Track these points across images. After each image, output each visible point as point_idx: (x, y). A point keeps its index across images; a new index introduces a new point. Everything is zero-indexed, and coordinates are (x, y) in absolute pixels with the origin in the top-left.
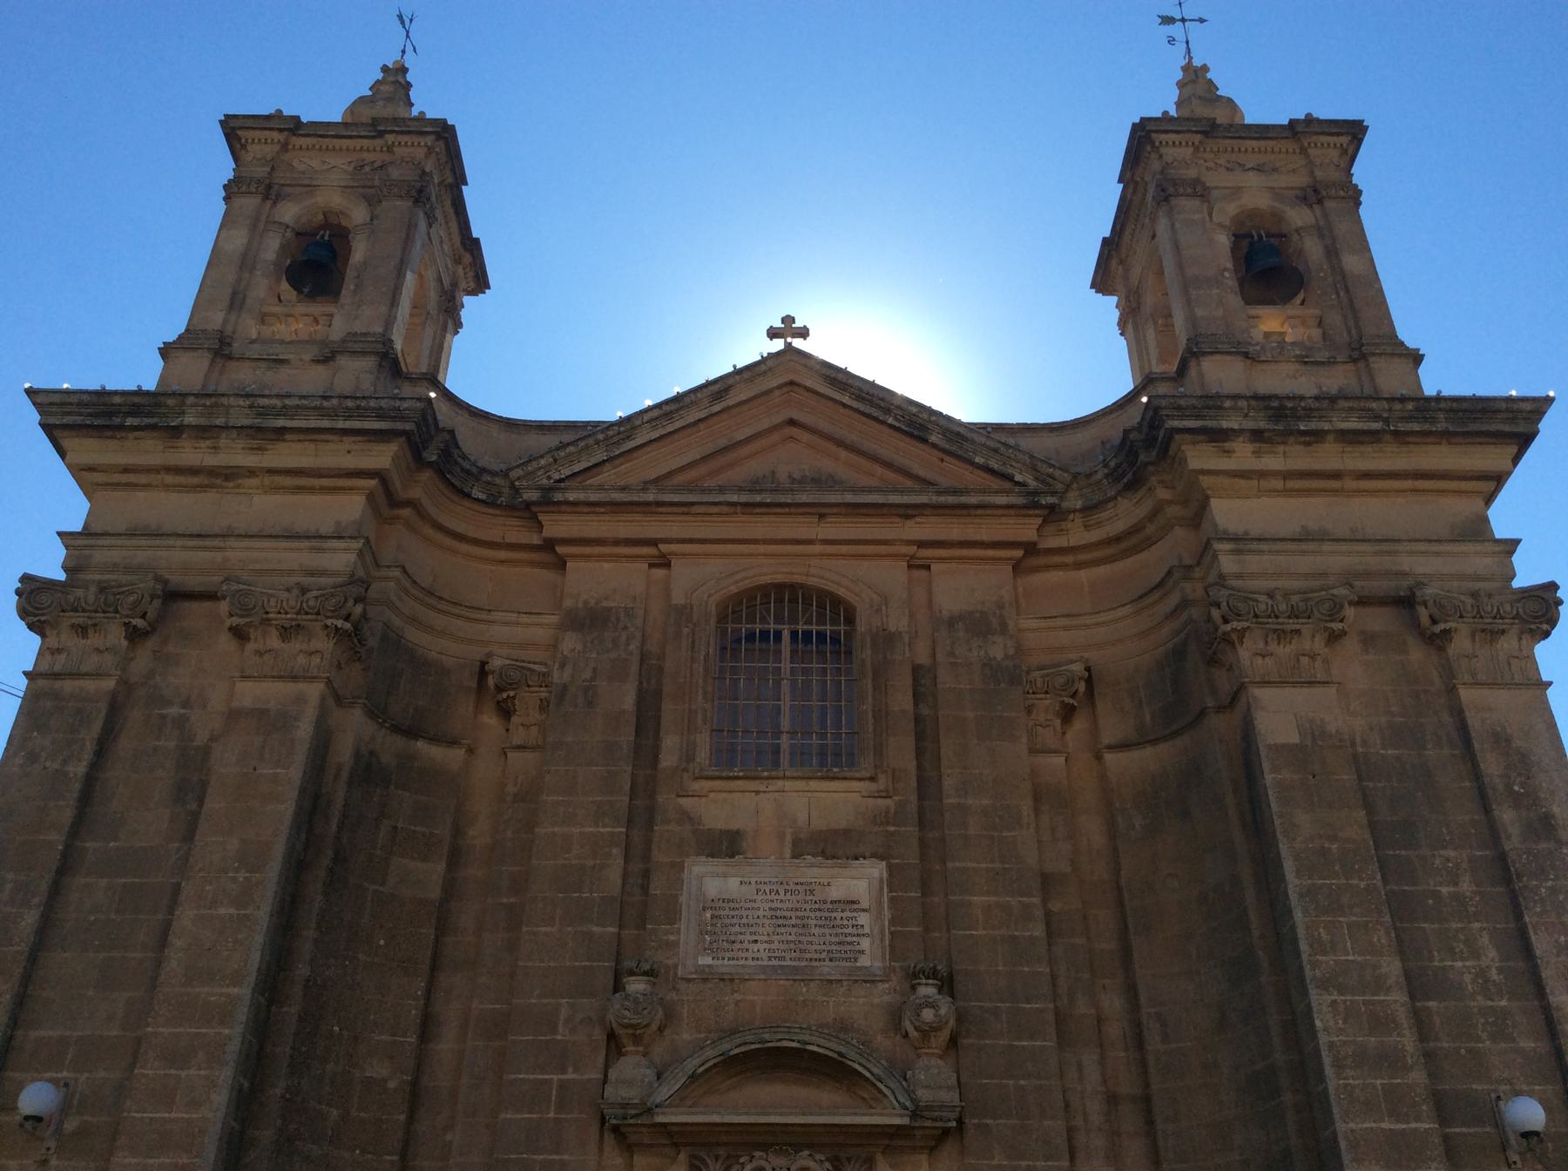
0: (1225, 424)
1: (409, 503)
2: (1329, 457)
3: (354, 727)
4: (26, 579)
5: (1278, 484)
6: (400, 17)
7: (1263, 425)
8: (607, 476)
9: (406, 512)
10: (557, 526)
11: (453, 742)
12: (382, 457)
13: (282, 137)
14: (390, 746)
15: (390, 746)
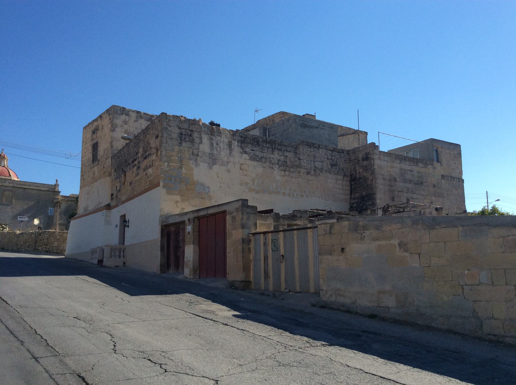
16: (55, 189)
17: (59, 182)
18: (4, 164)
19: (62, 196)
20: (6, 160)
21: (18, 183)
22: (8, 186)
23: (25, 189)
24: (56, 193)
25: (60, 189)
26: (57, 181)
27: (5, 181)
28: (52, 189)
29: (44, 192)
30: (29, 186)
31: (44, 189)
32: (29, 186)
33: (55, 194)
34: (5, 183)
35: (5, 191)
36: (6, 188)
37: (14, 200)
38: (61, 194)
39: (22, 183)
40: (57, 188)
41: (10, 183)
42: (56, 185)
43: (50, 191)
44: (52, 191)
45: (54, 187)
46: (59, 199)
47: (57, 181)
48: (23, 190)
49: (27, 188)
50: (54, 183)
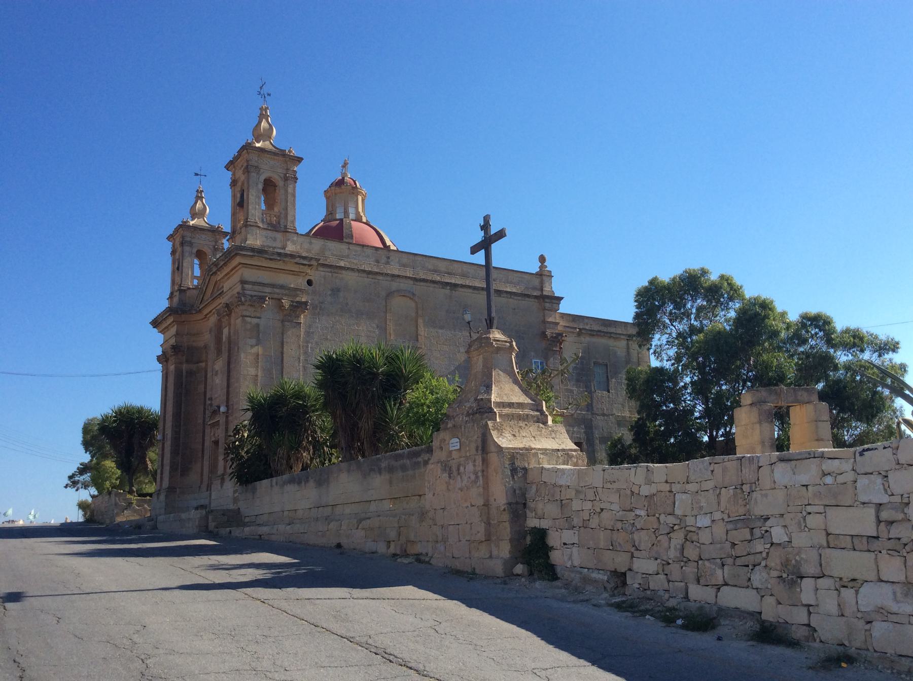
0: (214, 271)
1: (184, 321)
2: (226, 270)
3: (185, 367)
4: (157, 356)
5: (226, 278)
6: (196, 174)
7: (216, 269)
8: (205, 298)
9: (185, 322)
10: (206, 311)
11: (201, 362)
12: (171, 320)
13: (172, 238)
14: (194, 367)
15: (194, 367)
16: (542, 290)
17: (550, 265)
18: (357, 213)
19: (563, 315)
20: (360, 198)
21: (430, 267)
22: (399, 276)
23: (454, 286)
24: (547, 305)
25: (557, 287)
26: (542, 259)
27: (388, 258)
28: (534, 288)
29: (513, 302)
30: (464, 275)
31: (508, 290)
32: (464, 275)
33: (545, 309)
34: (387, 263)
35: (390, 295)
36: (395, 285)
37: (422, 331)
38: (564, 308)
39: (442, 267)
40: (547, 284)
41: (404, 266)
42: (543, 275)
43: (528, 296)
44: (536, 297)
45: (536, 282)
46: (557, 324)
47: (542, 259)
48: (447, 291)
49: (463, 286)
50: (534, 268)
